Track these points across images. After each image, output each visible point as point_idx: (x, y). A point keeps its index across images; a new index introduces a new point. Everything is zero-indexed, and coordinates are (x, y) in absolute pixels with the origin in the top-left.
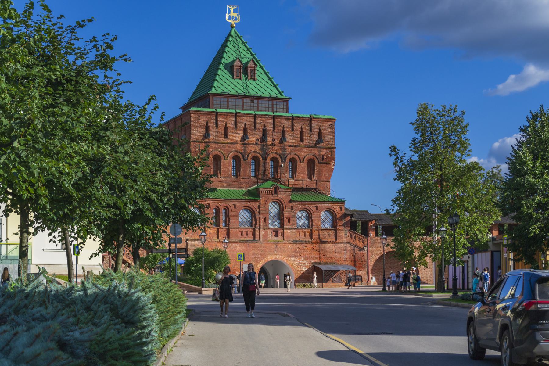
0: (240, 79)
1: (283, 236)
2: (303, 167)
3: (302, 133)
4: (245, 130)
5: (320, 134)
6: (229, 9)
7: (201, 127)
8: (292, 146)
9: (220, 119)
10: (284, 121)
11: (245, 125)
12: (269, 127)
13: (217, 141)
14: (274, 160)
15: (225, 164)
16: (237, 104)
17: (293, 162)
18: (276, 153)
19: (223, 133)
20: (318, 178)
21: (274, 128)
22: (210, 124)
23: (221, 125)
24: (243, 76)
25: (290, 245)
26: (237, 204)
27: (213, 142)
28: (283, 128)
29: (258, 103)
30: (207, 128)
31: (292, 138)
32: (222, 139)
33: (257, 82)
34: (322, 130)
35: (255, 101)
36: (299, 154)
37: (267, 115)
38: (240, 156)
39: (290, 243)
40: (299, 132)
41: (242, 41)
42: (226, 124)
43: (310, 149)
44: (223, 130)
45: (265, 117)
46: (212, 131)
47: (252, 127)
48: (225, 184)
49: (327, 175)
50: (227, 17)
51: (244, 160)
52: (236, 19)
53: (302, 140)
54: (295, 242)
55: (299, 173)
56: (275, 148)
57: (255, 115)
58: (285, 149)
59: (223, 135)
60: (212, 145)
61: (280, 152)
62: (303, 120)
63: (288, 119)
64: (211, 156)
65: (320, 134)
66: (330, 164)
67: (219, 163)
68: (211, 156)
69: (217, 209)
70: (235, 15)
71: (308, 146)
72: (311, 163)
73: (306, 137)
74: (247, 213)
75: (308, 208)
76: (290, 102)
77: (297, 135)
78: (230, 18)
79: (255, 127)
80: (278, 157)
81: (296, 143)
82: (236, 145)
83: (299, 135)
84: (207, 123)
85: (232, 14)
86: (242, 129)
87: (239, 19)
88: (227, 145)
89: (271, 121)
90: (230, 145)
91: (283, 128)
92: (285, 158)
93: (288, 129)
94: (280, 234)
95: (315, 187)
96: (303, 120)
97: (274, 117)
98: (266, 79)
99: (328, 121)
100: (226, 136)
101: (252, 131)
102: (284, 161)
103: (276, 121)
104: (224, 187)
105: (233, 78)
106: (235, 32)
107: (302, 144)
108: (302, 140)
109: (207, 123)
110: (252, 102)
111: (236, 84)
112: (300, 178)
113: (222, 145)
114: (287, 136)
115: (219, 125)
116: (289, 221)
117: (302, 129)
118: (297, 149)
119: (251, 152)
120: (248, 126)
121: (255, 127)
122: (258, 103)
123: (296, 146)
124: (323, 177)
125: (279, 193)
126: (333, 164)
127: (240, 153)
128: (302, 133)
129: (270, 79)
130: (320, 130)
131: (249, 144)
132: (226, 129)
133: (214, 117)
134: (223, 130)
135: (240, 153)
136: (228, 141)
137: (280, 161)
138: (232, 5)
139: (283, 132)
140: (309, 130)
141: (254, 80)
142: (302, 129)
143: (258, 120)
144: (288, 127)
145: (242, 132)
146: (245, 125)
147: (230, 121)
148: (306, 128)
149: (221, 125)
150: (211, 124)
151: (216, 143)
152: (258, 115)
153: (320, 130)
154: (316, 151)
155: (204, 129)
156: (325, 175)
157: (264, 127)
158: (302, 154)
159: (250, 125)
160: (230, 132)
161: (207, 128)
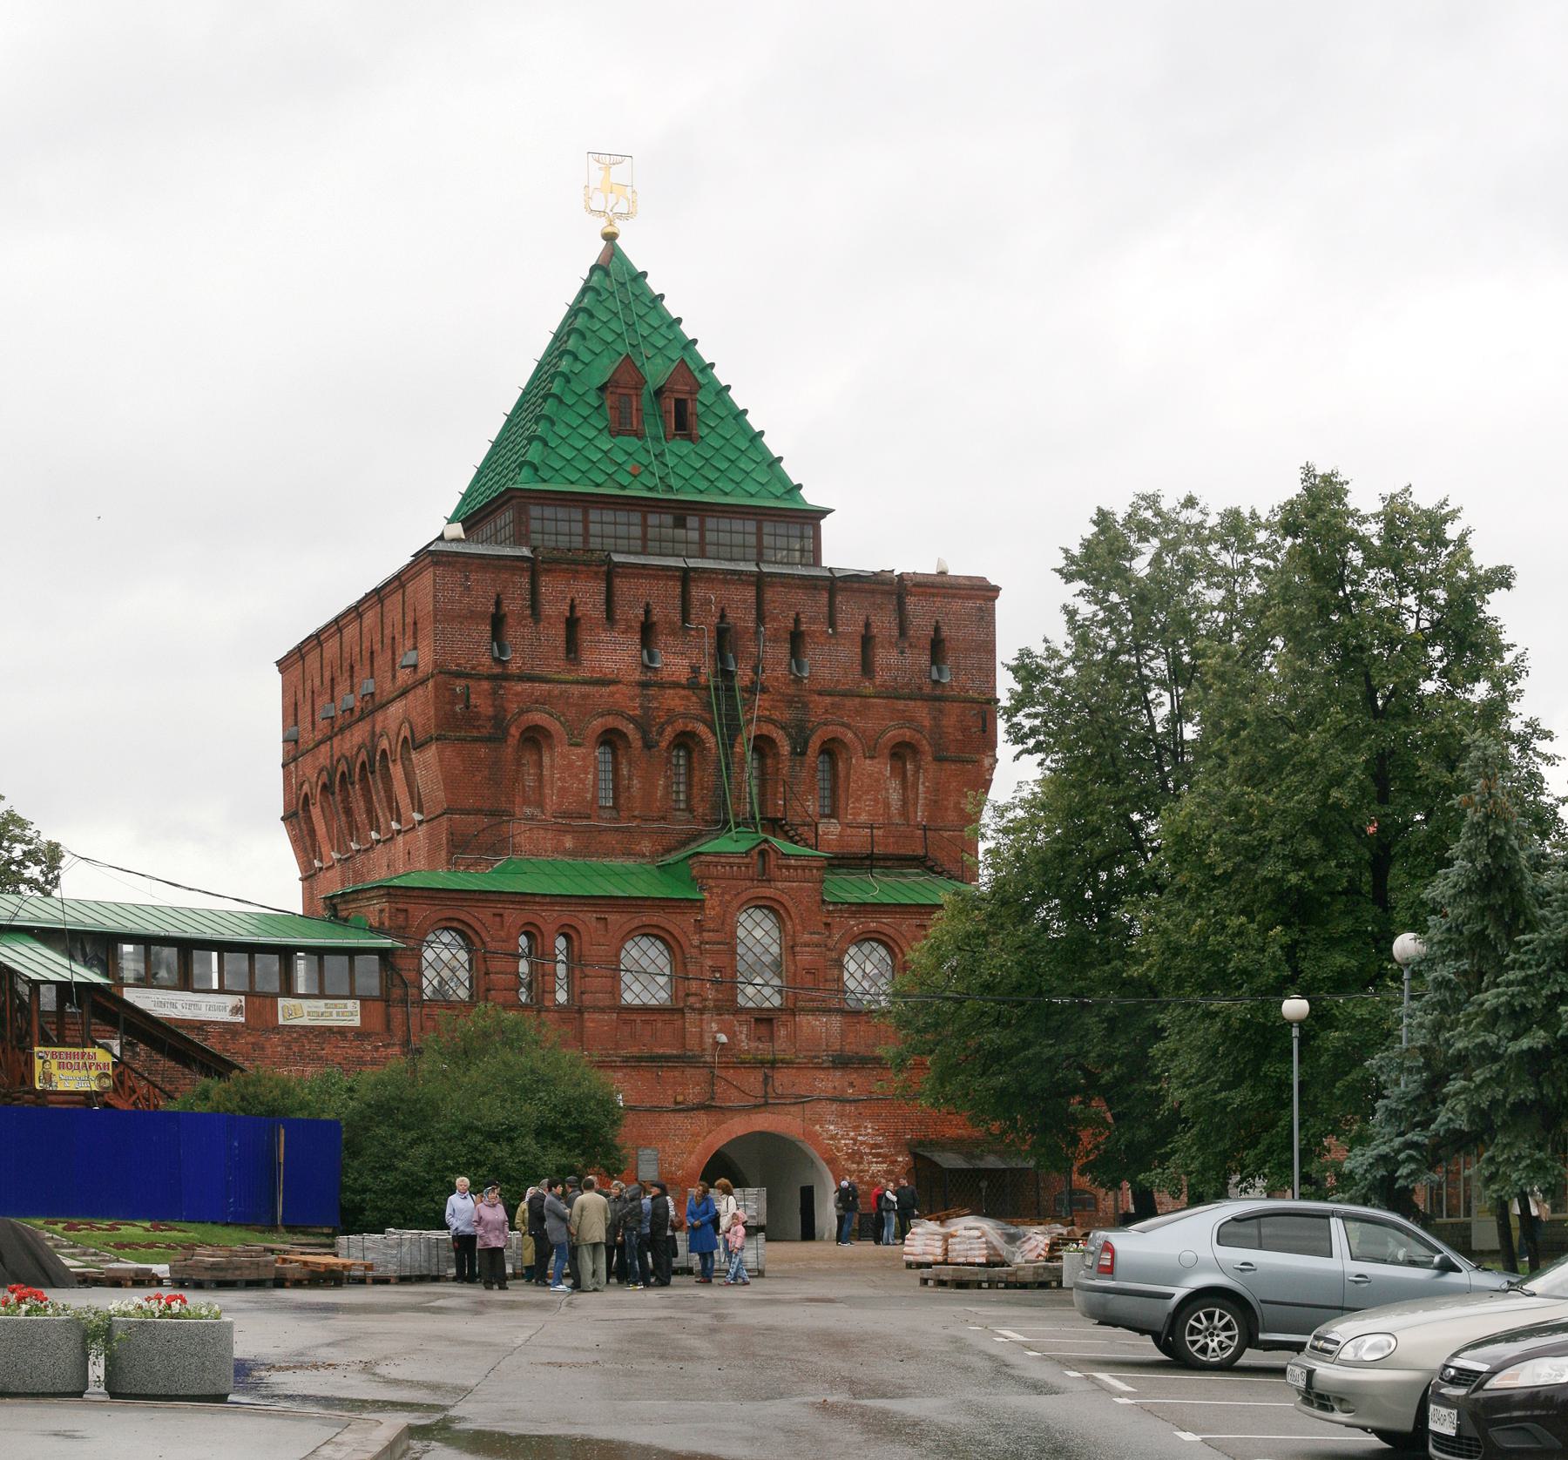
1: (793, 1037)
3: (867, 641)
7: (472, 616)
9: (547, 586)
10: (798, 597)
11: (647, 612)
12: (742, 617)
13: (537, 671)
14: (763, 746)
15: (571, 765)
16: (609, 530)
18: (769, 720)
19: (560, 642)
21: (760, 618)
22: (510, 607)
23: (554, 609)
26: (611, 917)
27: (522, 678)
28: (797, 621)
29: (702, 530)
30: (497, 622)
31: (830, 662)
32: (555, 665)
35: (693, 522)
36: (859, 723)
37: (734, 572)
38: (629, 729)
39: (819, 1067)
40: (859, 639)
42: (572, 607)
43: (901, 705)
45: (725, 582)
46: (512, 633)
47: (676, 617)
48: (569, 843)
51: (648, 745)
53: (867, 667)
54: (842, 1062)
55: (858, 800)
57: (686, 571)
58: (805, 705)
59: (561, 653)
60: (519, 687)
61: (787, 715)
62: (873, 592)
63: (815, 588)
64: (514, 731)
65: (937, 648)
66: (978, 762)
67: (546, 760)
68: (514, 731)
71: (892, 694)
73: (885, 657)
74: (653, 952)
75: (890, 931)
76: (824, 523)
77: (849, 653)
79: (685, 617)
80: (777, 734)
83: (858, 650)
84: (498, 604)
86: (637, 626)
88: (576, 690)
89: (750, 594)
91: (797, 621)
92: (806, 743)
95: (921, 852)
96: (873, 592)
97: (760, 582)
99: (970, 598)
103: (769, 595)
104: (566, 852)
107: (867, 687)
108: (867, 667)
109: (498, 604)
110: (680, 523)
112: (863, 818)
113: (557, 689)
115: (548, 609)
117: (867, 625)
119: (672, 717)
120: (657, 614)
121: (685, 617)
122: (702, 530)
126: (987, 762)
127: (631, 719)
128: (867, 641)
130: (937, 629)
131: (662, 686)
132: (572, 623)
133: (525, 581)
134: (558, 633)
135: (631, 719)
137: (785, 748)
139: (796, 639)
140: (896, 633)
142: (867, 625)
143: (697, 592)
144: (813, 620)
145: (637, 638)
146: (647, 612)
147: (589, 595)
148: (884, 624)
149: (554, 609)
150: (515, 605)
151: (532, 679)
152: (695, 569)
153: (937, 629)
154: (922, 712)
155: (486, 629)
157: (723, 617)
159: (666, 610)
160: (585, 638)
161: (497, 622)
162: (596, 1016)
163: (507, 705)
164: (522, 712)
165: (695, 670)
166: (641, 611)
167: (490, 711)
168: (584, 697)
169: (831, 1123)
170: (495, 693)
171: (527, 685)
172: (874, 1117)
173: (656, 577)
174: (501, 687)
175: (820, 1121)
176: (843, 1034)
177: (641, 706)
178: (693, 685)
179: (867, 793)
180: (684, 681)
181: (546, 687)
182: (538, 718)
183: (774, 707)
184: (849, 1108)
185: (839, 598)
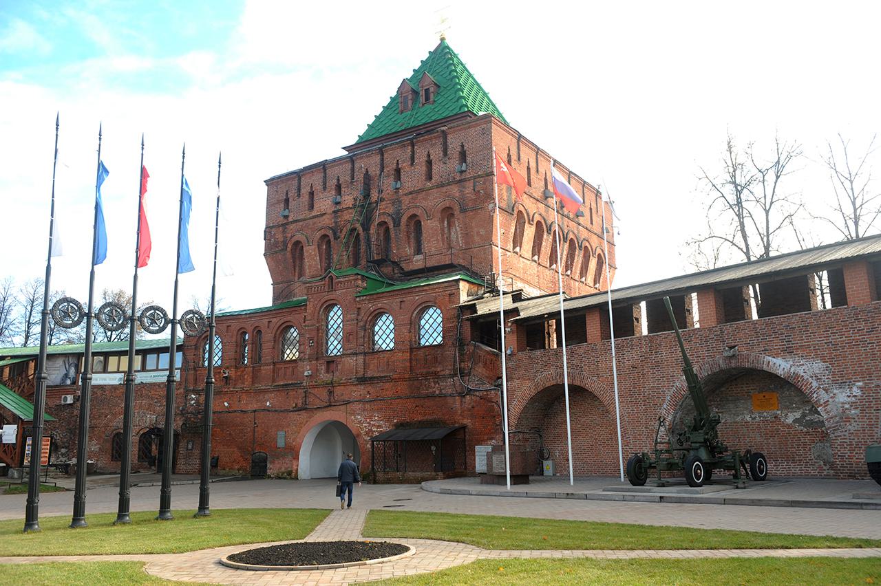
2: (430, 226)
4: (339, 188)
5: (463, 156)
8: (410, 193)
11: (338, 180)
15: (310, 255)
17: (416, 222)
20: (467, 243)
25: (354, 388)
28: (398, 164)
34: (466, 145)
36: (424, 204)
38: (330, 233)
43: (444, 189)
45: (367, 157)
46: (292, 204)
49: (482, 232)
51: (336, 238)
54: (362, 380)
55: (429, 241)
56: (382, 205)
65: (463, 156)
68: (290, 246)
72: (448, 213)
73: (437, 168)
77: (421, 169)
81: (419, 186)
82: (324, 217)
88: (311, 222)
90: (315, 220)
93: (405, 165)
100: (311, 207)
101: (348, 187)
102: (397, 223)
117: (429, 156)
118: (420, 196)
121: (353, 178)
123: (417, 192)
124: (476, 238)
132: (312, 194)
136: (314, 214)
142: (429, 156)
144: (404, 162)
145: (333, 192)
156: (478, 233)
158: (429, 204)
161: (287, 201)
162: (265, 367)
163: (287, 235)
164: (292, 237)
165: (355, 200)
166: (336, 180)
167: (282, 239)
168: (314, 224)
169: (358, 414)
170: (284, 231)
171: (294, 225)
172: (380, 410)
173: (341, 164)
174: (286, 228)
175: (354, 414)
176: (365, 366)
177: (334, 222)
178: (354, 205)
179: (432, 237)
180: (351, 206)
181: (301, 223)
182: (298, 237)
183: (387, 207)
184: (368, 406)
185: (416, 147)
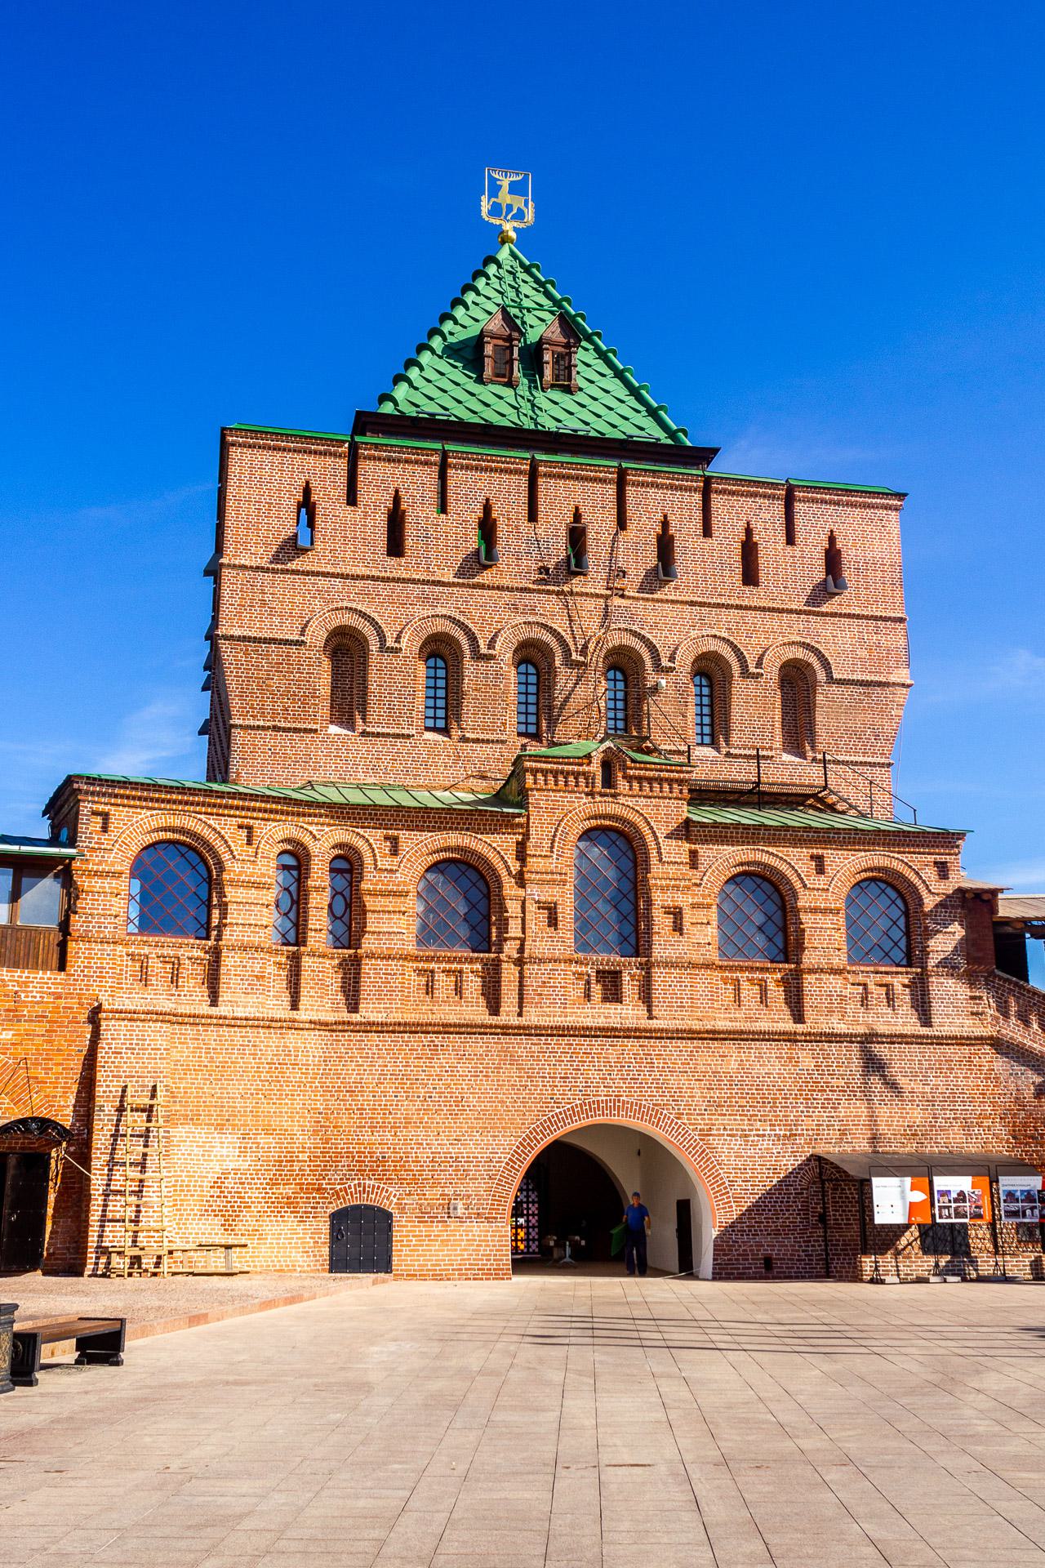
0: (510, 384)
5: (833, 559)
6: (493, 180)
24: (517, 373)
33: (580, 397)
41: (537, 281)
44: (381, 519)
50: (485, 205)
52: (520, 215)
69: (296, 861)
70: (518, 202)
78: (496, 210)
85: (505, 197)
87: (530, 216)
94: (629, 988)
98: (622, 392)
105: (480, 380)
106: (513, 254)
107: (751, 596)
111: (491, 399)
114: (682, 561)
116: (678, 928)
117: (749, 531)
125: (622, 785)
129: (634, 392)
138: (507, 166)
141: (568, 390)
